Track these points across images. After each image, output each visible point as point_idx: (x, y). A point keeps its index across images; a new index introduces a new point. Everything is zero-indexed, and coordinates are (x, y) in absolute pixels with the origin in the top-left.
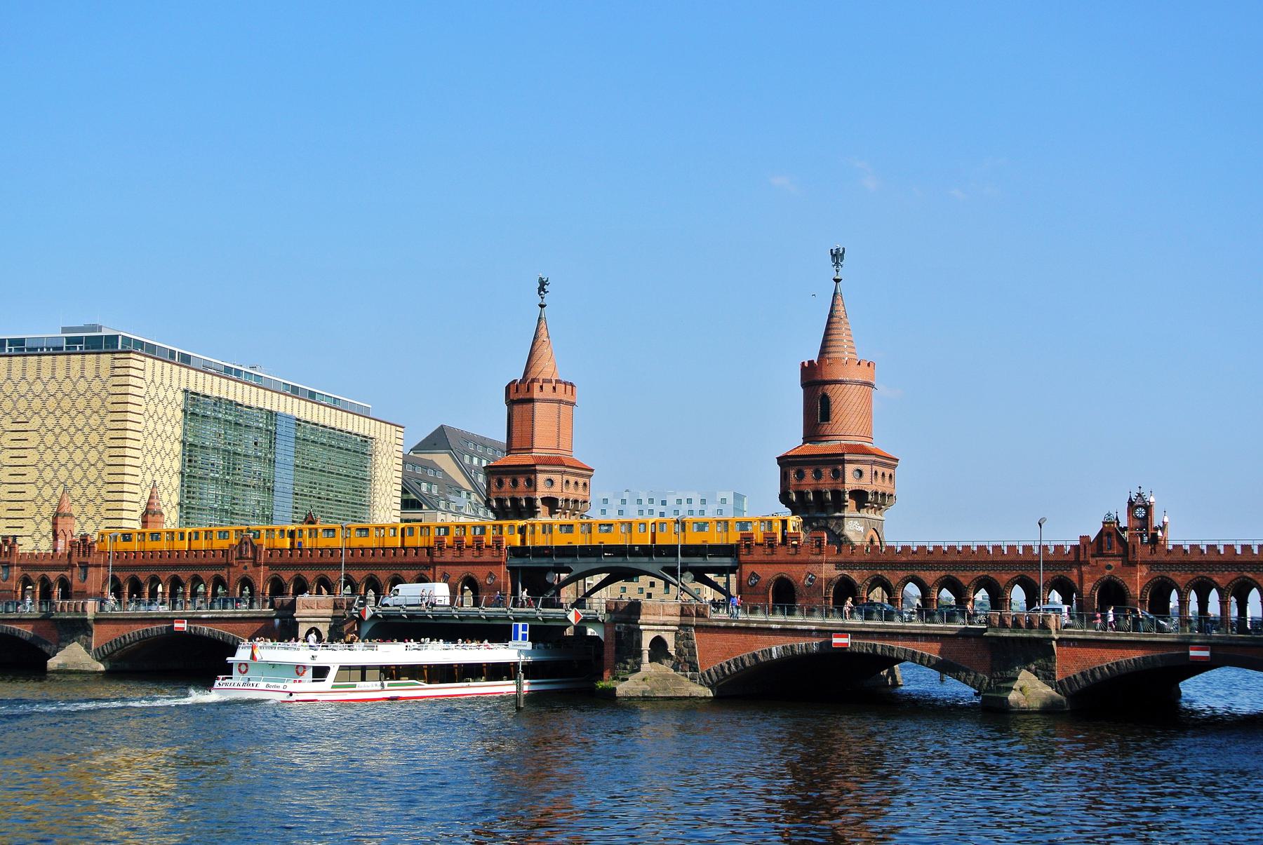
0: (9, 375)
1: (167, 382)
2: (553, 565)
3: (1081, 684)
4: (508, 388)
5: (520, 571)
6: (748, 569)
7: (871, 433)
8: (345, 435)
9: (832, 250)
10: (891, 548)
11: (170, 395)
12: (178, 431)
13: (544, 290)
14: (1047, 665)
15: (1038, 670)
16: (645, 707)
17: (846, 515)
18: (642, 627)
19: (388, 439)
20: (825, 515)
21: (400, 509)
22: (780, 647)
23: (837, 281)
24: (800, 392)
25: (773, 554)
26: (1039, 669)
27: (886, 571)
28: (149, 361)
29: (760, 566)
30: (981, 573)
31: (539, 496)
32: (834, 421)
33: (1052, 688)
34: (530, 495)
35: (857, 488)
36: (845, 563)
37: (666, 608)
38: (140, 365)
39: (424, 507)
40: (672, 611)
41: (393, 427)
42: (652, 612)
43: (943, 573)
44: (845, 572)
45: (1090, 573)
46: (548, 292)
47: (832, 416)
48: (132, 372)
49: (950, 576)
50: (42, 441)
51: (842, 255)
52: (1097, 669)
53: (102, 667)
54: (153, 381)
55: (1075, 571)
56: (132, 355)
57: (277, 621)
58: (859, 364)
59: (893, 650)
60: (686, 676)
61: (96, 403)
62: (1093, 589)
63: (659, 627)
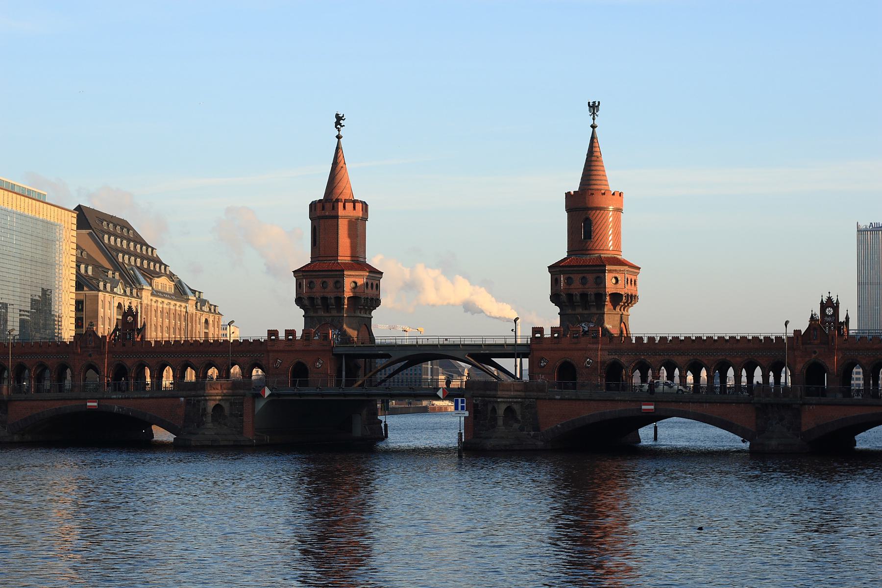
4: (311, 205)
5: (344, 357)
7: (620, 248)
9: (589, 103)
10: (639, 339)
13: (340, 124)
19: (66, 225)
21: (74, 291)
23: (593, 127)
24: (565, 215)
25: (559, 343)
34: (339, 295)
39: (85, 288)
41: (70, 213)
46: (344, 126)
47: (593, 235)
57: (182, 399)
60: (530, 435)
63: (511, 400)
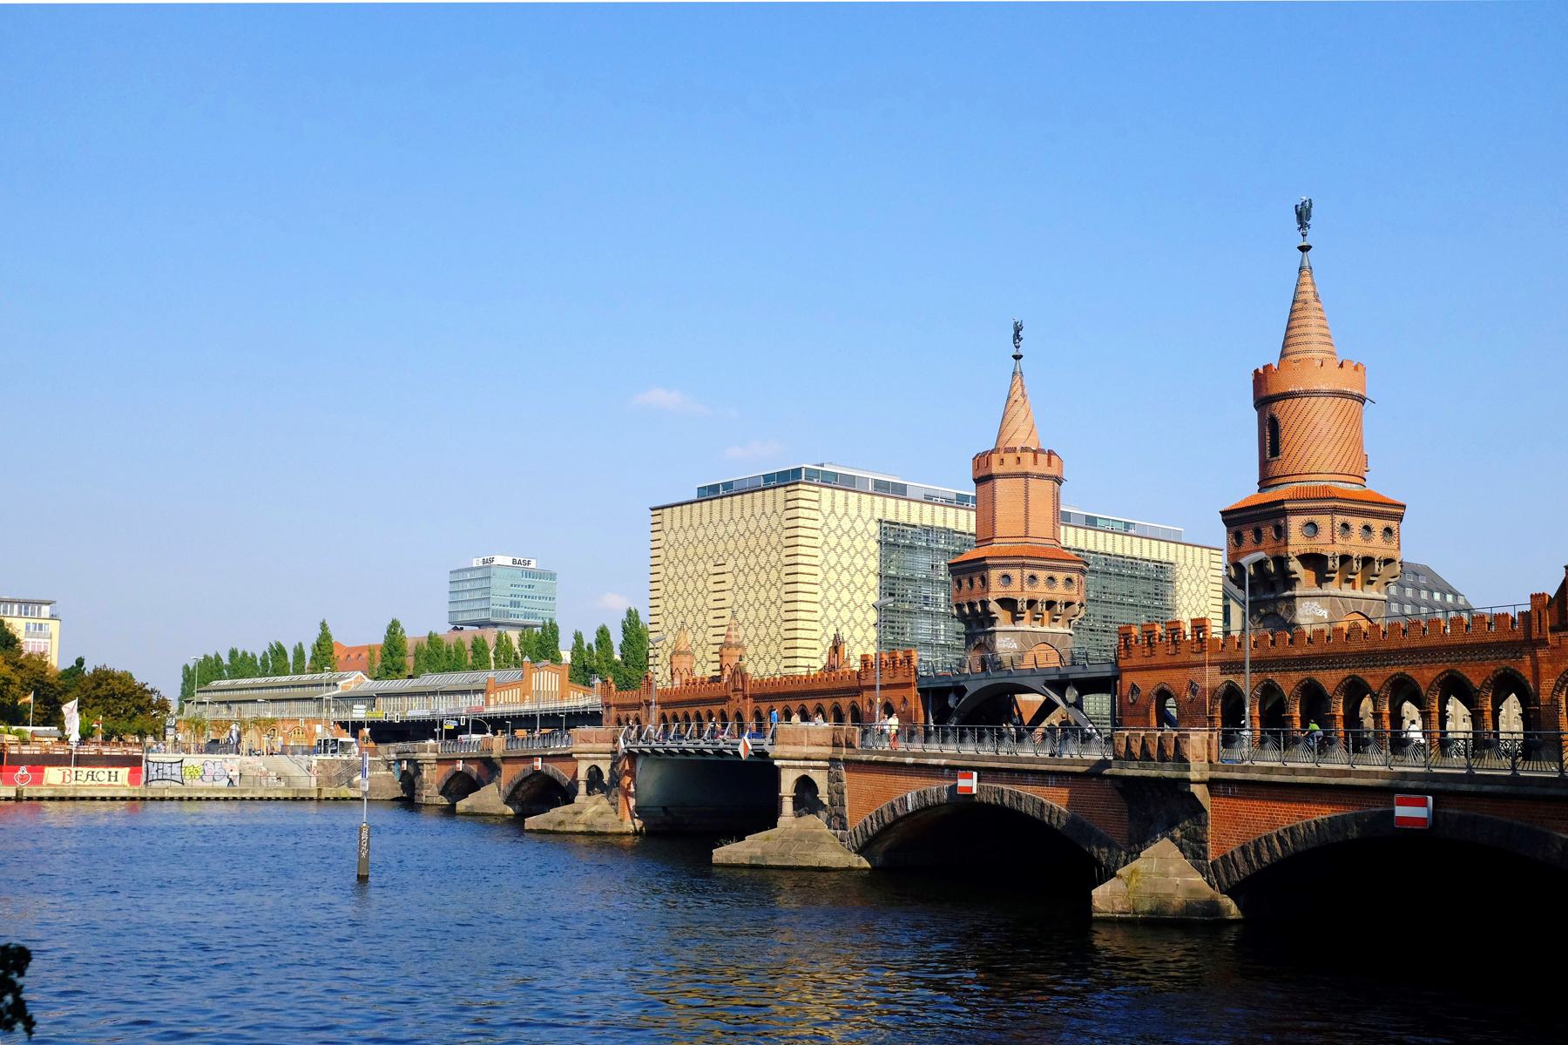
0: (711, 518)
1: (853, 512)
2: (951, 685)
3: (1241, 868)
6: (1128, 679)
8: (1134, 562)
11: (859, 525)
12: (874, 564)
13: (1018, 336)
14: (1195, 830)
15: (1184, 840)
16: (787, 883)
17: (1297, 593)
18: (777, 763)
19: (1198, 563)
20: (1272, 596)
22: (914, 793)
26: (1186, 838)
27: (1277, 674)
28: (826, 492)
29: (1139, 674)
30: (1396, 670)
31: (992, 597)
32: (1286, 453)
33: (1203, 876)
35: (1308, 552)
36: (1231, 663)
37: (811, 735)
38: (815, 496)
40: (819, 739)
42: (791, 740)
43: (1346, 673)
44: (1231, 678)
45: (1550, 661)
48: (801, 503)
49: (1354, 676)
50: (736, 583)
51: (1309, 211)
52: (1263, 840)
53: (510, 811)
54: (833, 511)
55: (1527, 658)
56: (800, 486)
58: (1341, 366)
59: (1019, 798)
61: (774, 539)
62: (1555, 689)
63: (802, 763)
